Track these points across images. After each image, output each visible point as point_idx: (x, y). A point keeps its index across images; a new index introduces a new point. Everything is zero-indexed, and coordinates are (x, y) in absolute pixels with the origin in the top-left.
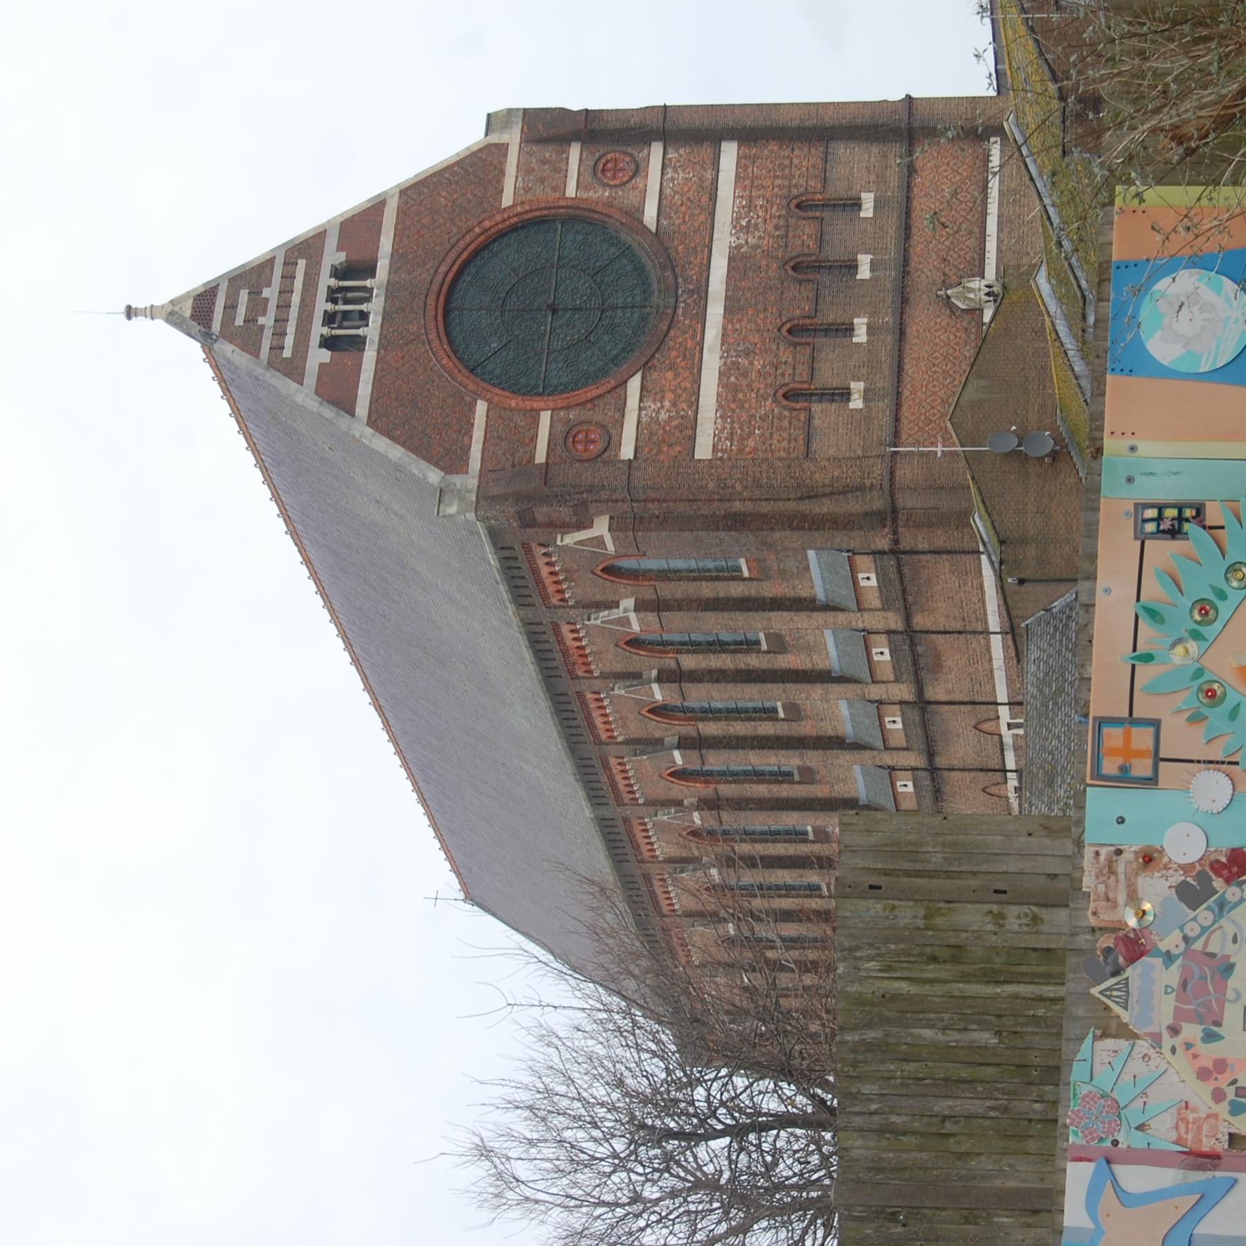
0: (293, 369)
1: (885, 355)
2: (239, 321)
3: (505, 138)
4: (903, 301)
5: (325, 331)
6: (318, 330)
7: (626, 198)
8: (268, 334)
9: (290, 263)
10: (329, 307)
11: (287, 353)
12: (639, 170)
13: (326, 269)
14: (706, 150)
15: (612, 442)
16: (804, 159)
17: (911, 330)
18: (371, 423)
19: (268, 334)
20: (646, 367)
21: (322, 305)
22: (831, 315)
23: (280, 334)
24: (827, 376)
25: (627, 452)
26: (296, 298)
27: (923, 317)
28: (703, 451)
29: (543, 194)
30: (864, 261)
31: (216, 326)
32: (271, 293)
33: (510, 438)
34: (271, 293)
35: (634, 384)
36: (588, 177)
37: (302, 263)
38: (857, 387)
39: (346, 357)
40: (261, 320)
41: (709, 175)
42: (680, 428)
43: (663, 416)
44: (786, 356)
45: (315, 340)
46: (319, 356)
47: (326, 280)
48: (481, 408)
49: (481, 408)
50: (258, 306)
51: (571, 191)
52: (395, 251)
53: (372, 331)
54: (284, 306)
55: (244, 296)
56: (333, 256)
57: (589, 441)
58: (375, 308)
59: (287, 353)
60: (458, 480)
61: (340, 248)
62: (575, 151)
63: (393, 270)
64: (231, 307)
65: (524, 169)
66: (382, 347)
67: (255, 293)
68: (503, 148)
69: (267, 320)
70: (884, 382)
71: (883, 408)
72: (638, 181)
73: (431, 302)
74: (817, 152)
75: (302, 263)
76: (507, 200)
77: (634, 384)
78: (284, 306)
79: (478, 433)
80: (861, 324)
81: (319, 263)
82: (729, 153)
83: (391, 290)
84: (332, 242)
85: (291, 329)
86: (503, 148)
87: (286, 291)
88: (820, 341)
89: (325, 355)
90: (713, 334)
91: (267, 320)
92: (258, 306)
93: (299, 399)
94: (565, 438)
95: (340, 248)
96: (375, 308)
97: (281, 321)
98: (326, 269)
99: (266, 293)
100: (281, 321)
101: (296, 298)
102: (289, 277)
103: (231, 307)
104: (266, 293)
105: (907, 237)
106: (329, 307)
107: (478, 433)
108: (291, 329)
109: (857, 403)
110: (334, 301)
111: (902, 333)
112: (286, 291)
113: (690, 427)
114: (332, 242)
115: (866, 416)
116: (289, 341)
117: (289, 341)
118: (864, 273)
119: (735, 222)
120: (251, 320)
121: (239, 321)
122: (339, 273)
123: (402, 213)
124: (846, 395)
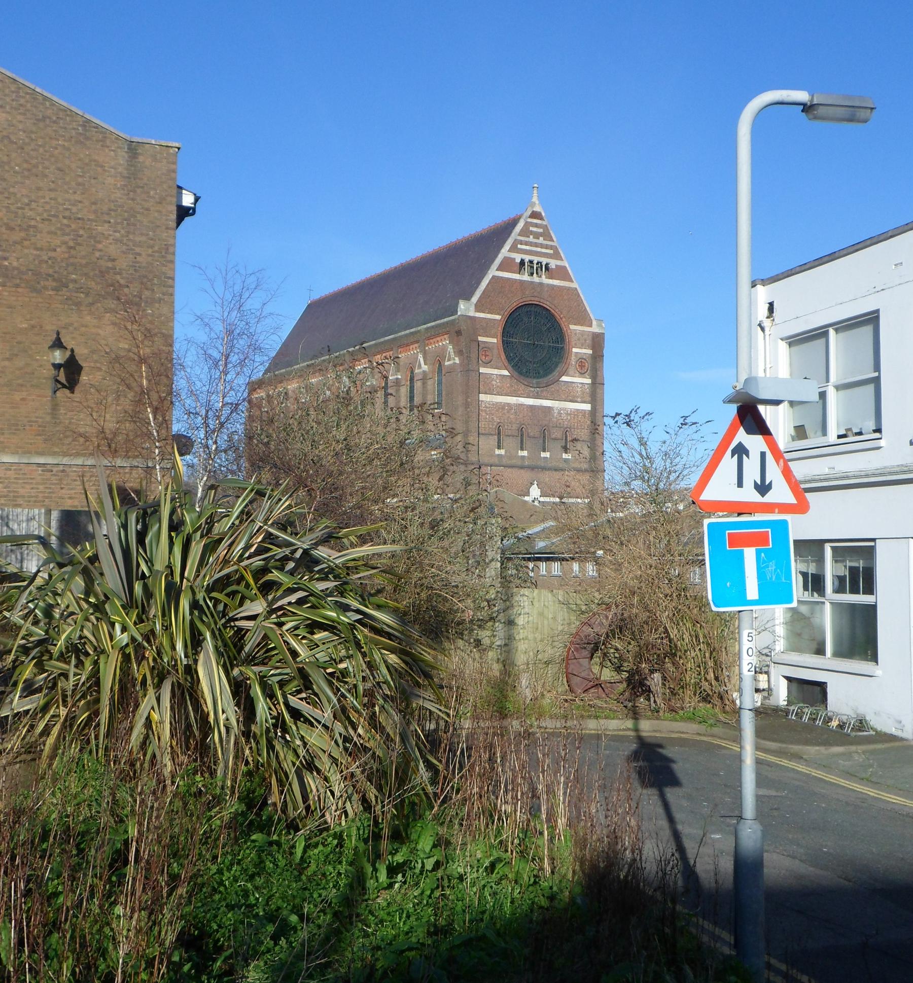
0: (514, 249)
1: (514, 462)
2: (531, 228)
4: (532, 468)
6: (527, 258)
7: (571, 370)
9: (551, 247)
10: (535, 262)
11: (519, 246)
12: (582, 374)
14: (589, 399)
15: (487, 364)
16: (583, 433)
17: (522, 471)
18: (494, 277)
20: (512, 376)
21: (536, 259)
22: (528, 443)
23: (526, 244)
24: (507, 441)
25: (482, 370)
26: (539, 249)
27: (526, 475)
28: (482, 397)
29: (573, 340)
30: (547, 455)
31: (529, 220)
33: (486, 327)
35: (506, 373)
36: (579, 356)
37: (551, 252)
38: (502, 452)
39: (517, 268)
41: (579, 400)
42: (490, 389)
43: (494, 383)
44: (515, 427)
46: (518, 258)
47: (544, 261)
48: (498, 317)
49: (498, 317)
50: (537, 236)
51: (574, 350)
53: (526, 277)
54: (536, 245)
55: (541, 230)
56: (553, 263)
57: (486, 356)
58: (535, 278)
59: (519, 246)
60: (473, 308)
62: (590, 352)
63: (548, 285)
64: (536, 225)
65: (583, 332)
66: (522, 282)
67: (541, 235)
68: (591, 326)
69: (531, 239)
70: (504, 461)
71: (496, 461)
72: (578, 374)
73: (536, 299)
74: (586, 438)
75: (551, 252)
76: (572, 327)
77: (506, 373)
78: (536, 245)
79: (489, 316)
80: (525, 453)
81: (551, 258)
82: (587, 407)
83: (541, 284)
84: (559, 263)
85: (528, 248)
86: (591, 326)
87: (542, 246)
88: (519, 438)
89: (518, 260)
90: (522, 400)
91: (531, 239)
92: (537, 236)
93: (503, 251)
94: (487, 347)
96: (535, 278)
97: (531, 244)
98: (548, 260)
99: (541, 238)
100: (531, 244)
101: (539, 249)
102: (547, 247)
103: (536, 225)
104: (541, 238)
105: (556, 470)
106: (535, 262)
107: (489, 316)
108: (528, 248)
109: (497, 452)
110: (537, 264)
111: (522, 467)
112: (542, 246)
113: (489, 392)
114: (559, 263)
115: (493, 455)
116: (524, 247)
117: (524, 247)
118: (543, 455)
119: (564, 409)
120: (532, 233)
121: (531, 228)
122: (547, 265)
123: (569, 289)
124: (499, 448)
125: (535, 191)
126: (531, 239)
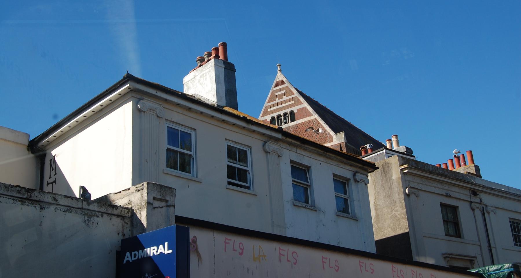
3: (334, 140)
5: (276, 116)
6: (275, 115)
8: (274, 102)
11: (269, 110)
13: (291, 109)
19: (274, 102)
21: (282, 113)
32: (285, 98)
34: (285, 98)
37: (293, 102)
40: (277, 99)
45: (272, 115)
47: (288, 111)
50: (280, 97)
52: (298, 125)
56: (295, 109)
59: (269, 110)
61: (298, 110)
63: (293, 127)
64: (280, 90)
69: (278, 101)
78: (281, 103)
85: (276, 107)
87: (285, 102)
92: (280, 97)
95: (298, 110)
103: (280, 90)
104: (285, 97)
112: (285, 102)
116: (272, 109)
117: (272, 109)
121: (277, 94)
122: (292, 113)
125: (279, 68)
126: (278, 101)
